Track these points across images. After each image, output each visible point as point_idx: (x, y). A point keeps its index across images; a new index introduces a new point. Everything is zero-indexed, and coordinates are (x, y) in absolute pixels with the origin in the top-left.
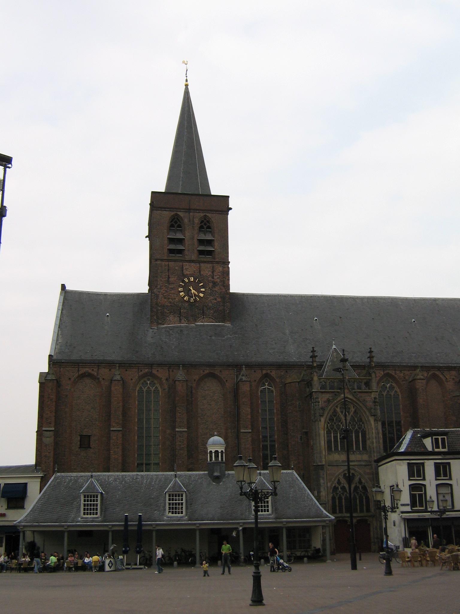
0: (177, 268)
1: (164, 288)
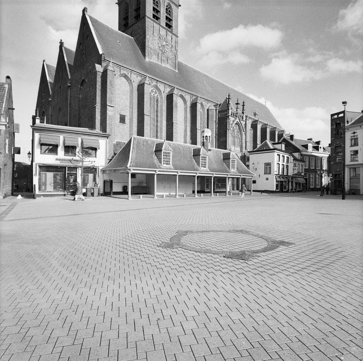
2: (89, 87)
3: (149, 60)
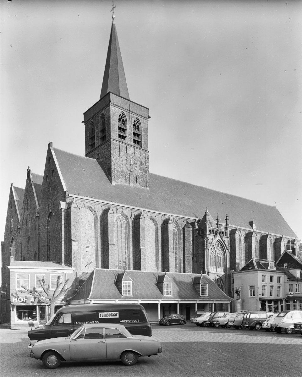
0: (124, 148)
2: (56, 221)
3: (116, 183)
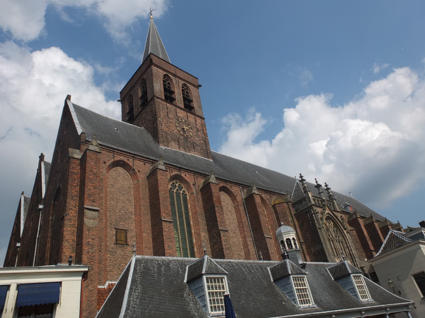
0: (172, 109)
1: (165, 120)
